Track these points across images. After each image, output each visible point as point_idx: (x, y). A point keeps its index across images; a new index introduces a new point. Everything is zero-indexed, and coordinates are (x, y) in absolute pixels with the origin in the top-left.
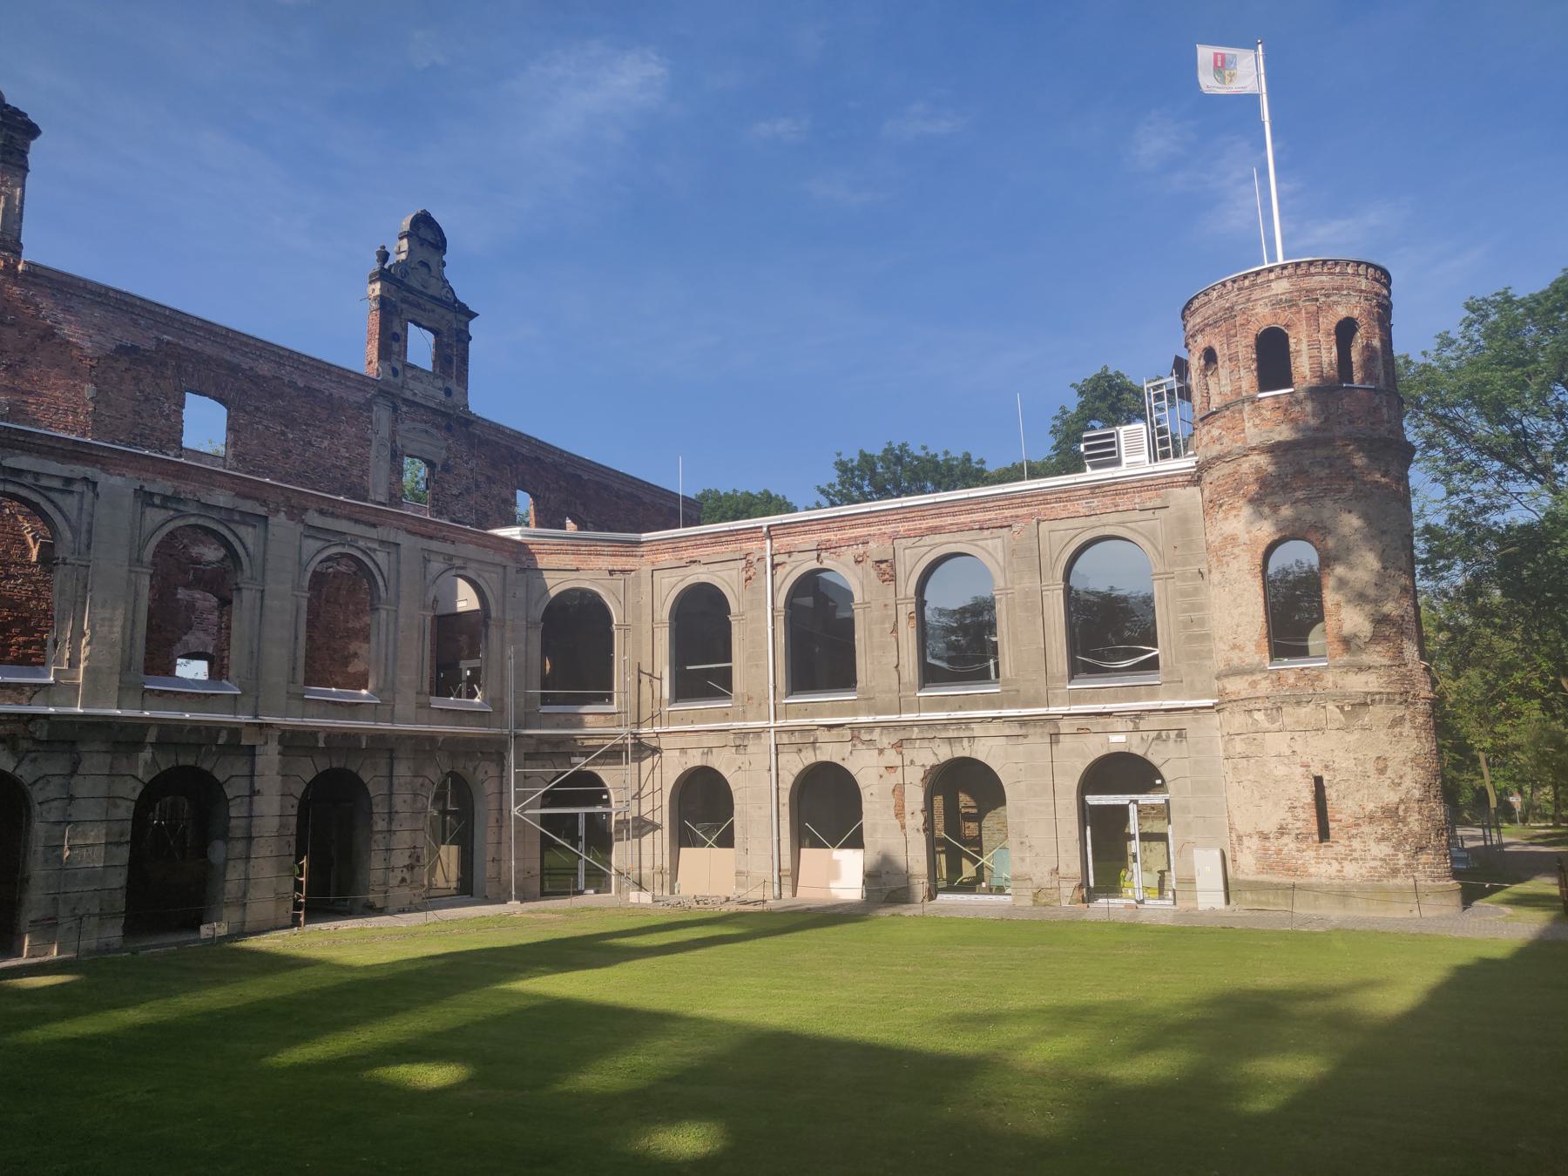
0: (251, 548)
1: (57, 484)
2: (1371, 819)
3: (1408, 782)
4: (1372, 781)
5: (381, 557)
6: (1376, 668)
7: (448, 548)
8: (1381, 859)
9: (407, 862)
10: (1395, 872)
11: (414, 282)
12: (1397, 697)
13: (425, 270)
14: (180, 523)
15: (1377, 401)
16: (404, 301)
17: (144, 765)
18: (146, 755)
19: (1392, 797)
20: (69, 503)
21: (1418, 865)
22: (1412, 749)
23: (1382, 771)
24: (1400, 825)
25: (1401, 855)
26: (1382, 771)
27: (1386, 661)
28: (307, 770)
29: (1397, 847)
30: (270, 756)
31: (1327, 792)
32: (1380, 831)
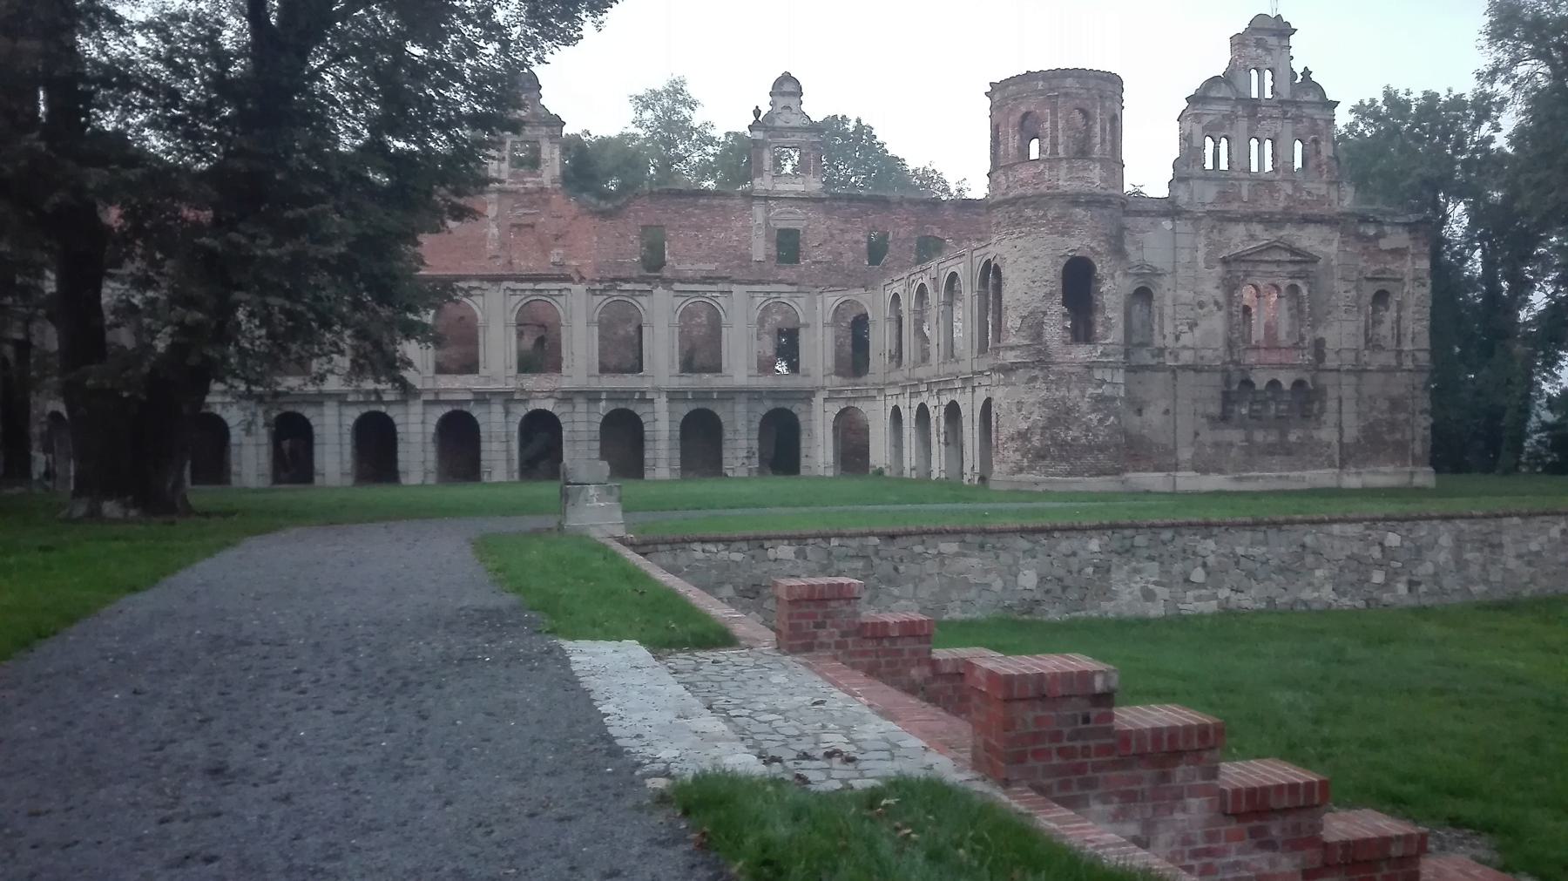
0: (645, 305)
1: (556, 293)
3: (1035, 417)
5: (721, 300)
7: (766, 288)
9: (745, 455)
10: (1021, 470)
11: (779, 123)
14: (610, 300)
16: (770, 137)
17: (604, 407)
18: (603, 404)
19: (1024, 426)
20: (561, 300)
23: (1019, 410)
26: (1019, 410)
27: (1027, 342)
28: (684, 409)
29: (1023, 456)
30: (662, 403)
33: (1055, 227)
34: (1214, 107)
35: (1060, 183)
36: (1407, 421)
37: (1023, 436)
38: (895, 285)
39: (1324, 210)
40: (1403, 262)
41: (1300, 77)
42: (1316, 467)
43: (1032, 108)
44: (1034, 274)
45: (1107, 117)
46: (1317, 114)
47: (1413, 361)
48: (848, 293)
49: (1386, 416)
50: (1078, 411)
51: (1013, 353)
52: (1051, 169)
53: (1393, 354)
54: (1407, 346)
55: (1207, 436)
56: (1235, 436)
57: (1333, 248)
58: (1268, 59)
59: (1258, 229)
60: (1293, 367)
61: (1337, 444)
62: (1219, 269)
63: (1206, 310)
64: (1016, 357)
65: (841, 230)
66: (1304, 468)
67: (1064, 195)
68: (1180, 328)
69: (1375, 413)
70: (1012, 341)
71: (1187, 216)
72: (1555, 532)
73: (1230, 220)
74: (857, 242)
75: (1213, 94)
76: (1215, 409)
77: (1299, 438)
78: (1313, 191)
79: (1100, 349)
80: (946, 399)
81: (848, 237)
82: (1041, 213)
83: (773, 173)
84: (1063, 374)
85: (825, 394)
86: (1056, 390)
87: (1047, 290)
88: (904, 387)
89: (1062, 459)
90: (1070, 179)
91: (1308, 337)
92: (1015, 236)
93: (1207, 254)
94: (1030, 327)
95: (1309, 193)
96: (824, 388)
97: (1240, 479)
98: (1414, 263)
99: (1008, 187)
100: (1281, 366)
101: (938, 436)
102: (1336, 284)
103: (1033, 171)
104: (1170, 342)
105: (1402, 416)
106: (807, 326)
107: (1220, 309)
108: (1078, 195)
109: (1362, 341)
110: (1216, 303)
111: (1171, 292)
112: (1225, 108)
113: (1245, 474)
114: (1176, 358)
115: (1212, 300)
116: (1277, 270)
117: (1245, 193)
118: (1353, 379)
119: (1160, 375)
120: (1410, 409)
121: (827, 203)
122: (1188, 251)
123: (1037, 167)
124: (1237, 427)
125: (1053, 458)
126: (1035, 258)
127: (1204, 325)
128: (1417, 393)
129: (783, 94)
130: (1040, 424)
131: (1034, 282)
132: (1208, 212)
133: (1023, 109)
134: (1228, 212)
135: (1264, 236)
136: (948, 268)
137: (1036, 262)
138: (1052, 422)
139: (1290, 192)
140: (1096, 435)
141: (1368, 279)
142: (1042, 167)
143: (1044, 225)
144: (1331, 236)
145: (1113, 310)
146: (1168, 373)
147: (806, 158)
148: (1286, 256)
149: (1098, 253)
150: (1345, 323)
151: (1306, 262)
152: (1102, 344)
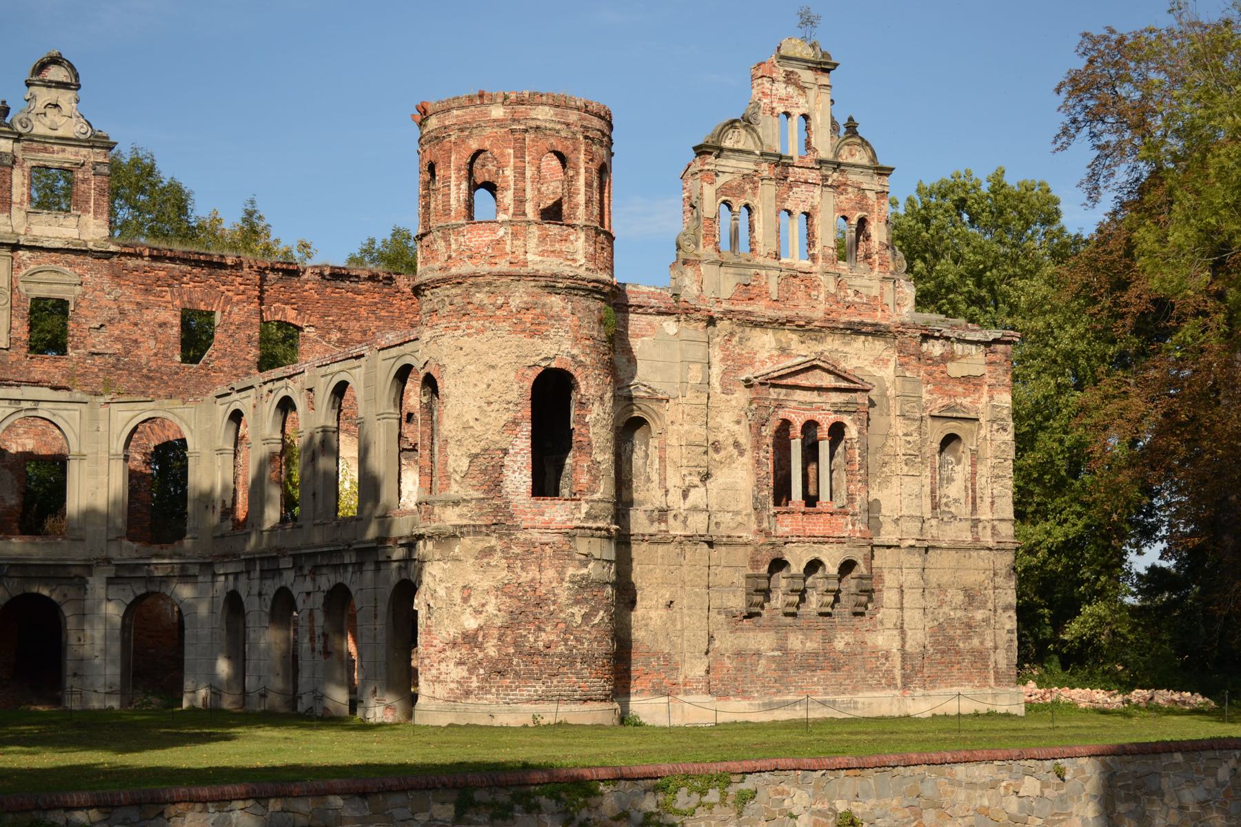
2: (454, 644)
3: (491, 609)
4: (457, 608)
6: (468, 501)
8: (458, 682)
10: (468, 693)
12: (484, 529)
13: (55, 111)
15: (501, 232)
16: (24, 149)
19: (471, 623)
21: (490, 687)
22: (499, 577)
24: (476, 651)
25: (474, 678)
26: (465, 600)
29: (471, 671)
31: (185, 618)
32: (458, 656)
33: (521, 321)
34: (732, 162)
35: (530, 257)
36: (986, 620)
37: (470, 639)
38: (235, 396)
39: (879, 318)
40: (977, 396)
41: (843, 130)
42: (871, 688)
43: (487, 145)
44: (488, 393)
45: (594, 167)
46: (871, 183)
47: (993, 534)
48: (151, 405)
49: (959, 613)
50: (554, 603)
51: (457, 510)
52: (515, 235)
53: (967, 525)
54: (985, 514)
55: (726, 642)
56: (761, 641)
57: (888, 373)
58: (802, 100)
59: (792, 338)
60: (840, 541)
61: (899, 654)
62: (741, 396)
63: (723, 453)
64: (460, 516)
65: (138, 304)
66: (855, 689)
67: (535, 276)
68: (688, 479)
69: (946, 609)
70: (455, 490)
71: (698, 315)
72: (1223, 773)
73: (757, 325)
74: (163, 325)
75: (727, 144)
76: (738, 602)
77: (847, 644)
78: (862, 290)
79: (585, 508)
80: (326, 581)
81: (148, 315)
82: (500, 301)
83: (26, 206)
84: (533, 543)
85: (110, 571)
86: (522, 568)
87: (507, 416)
88: (250, 561)
89: (532, 677)
90: (542, 253)
91: (858, 498)
92: (460, 332)
93: (724, 373)
94: (484, 472)
95: (857, 292)
96: (108, 561)
97: (770, 707)
98: (992, 398)
99: (450, 257)
100: (824, 540)
101: (312, 640)
102: (893, 422)
103: (487, 237)
104: (674, 499)
105: (979, 615)
106: (82, 457)
107: (741, 453)
108: (555, 276)
109: (927, 503)
110: (736, 444)
111: (675, 427)
112: (747, 166)
113: (777, 699)
114: (685, 521)
115: (731, 440)
116: (817, 399)
117: (773, 288)
118: (917, 559)
119: (661, 549)
120: (990, 605)
121: (115, 259)
122: (699, 366)
123: (494, 231)
124: (762, 628)
125: (517, 674)
126: (493, 367)
127: (721, 478)
128: (999, 580)
129: (49, 85)
130: (498, 622)
131: (489, 403)
132: (726, 313)
133: (474, 145)
134: (748, 313)
135: (802, 351)
136: (334, 374)
137: (492, 374)
138: (514, 620)
139: (833, 290)
140: (576, 639)
141: (933, 417)
142: (501, 232)
143: (506, 319)
144: (885, 355)
145: (603, 451)
146: (671, 547)
147: (83, 187)
148: (828, 381)
149: (581, 364)
150: (907, 479)
151: (855, 391)
152: (587, 502)
